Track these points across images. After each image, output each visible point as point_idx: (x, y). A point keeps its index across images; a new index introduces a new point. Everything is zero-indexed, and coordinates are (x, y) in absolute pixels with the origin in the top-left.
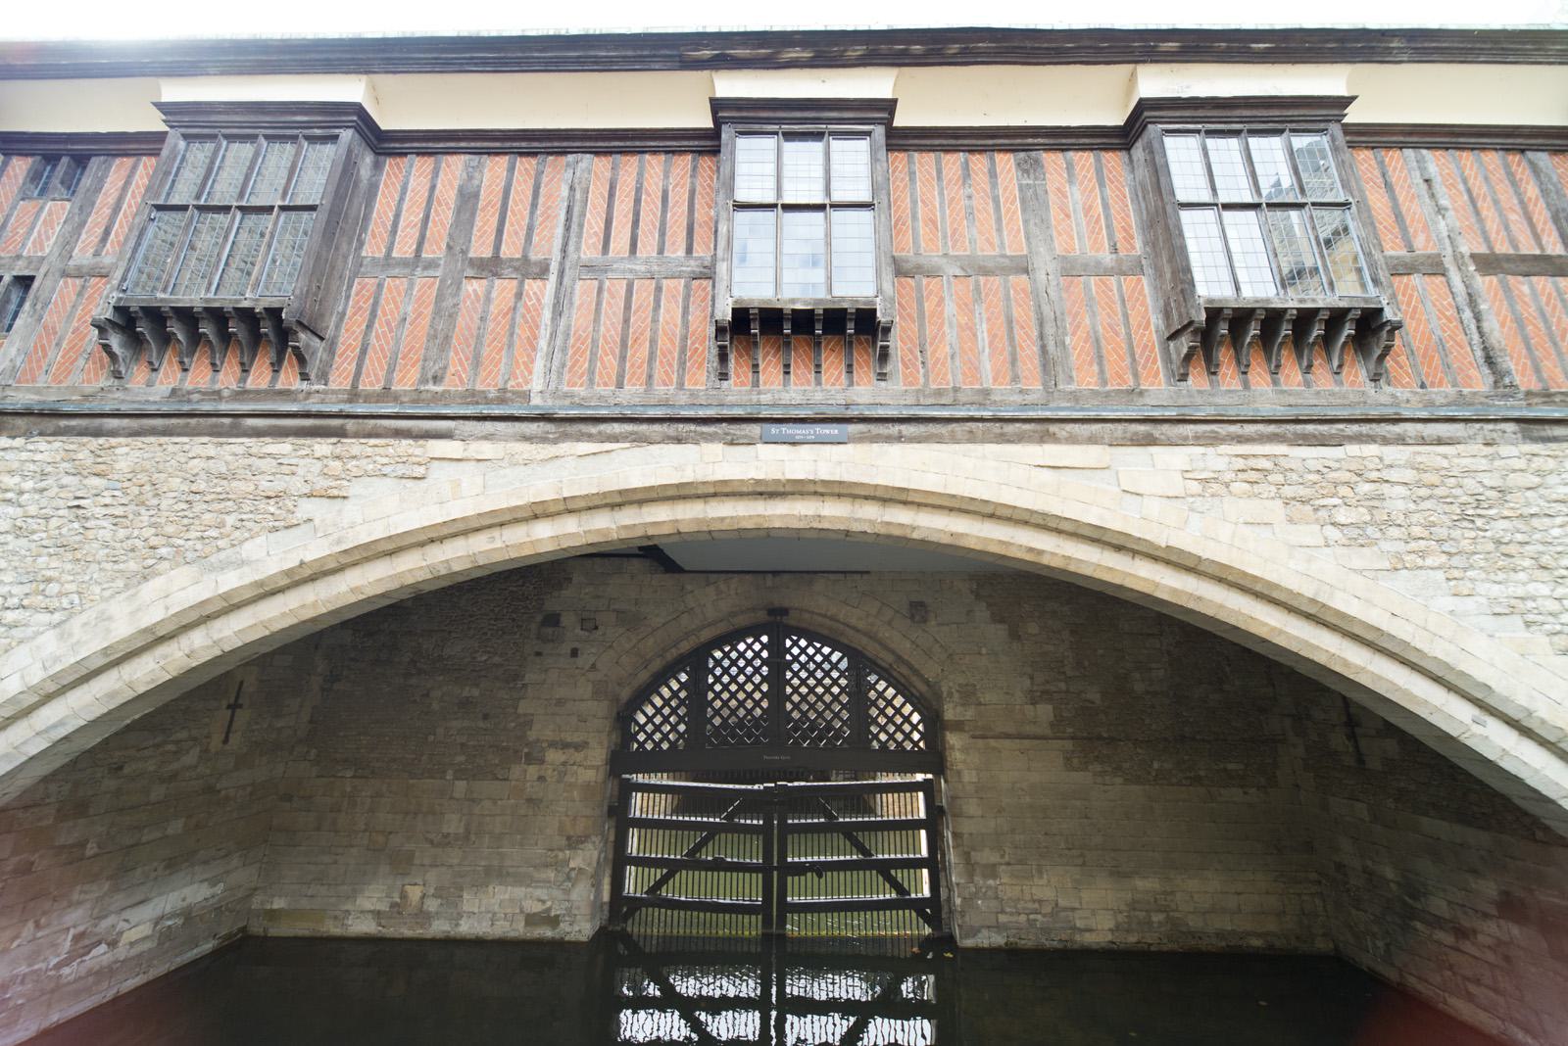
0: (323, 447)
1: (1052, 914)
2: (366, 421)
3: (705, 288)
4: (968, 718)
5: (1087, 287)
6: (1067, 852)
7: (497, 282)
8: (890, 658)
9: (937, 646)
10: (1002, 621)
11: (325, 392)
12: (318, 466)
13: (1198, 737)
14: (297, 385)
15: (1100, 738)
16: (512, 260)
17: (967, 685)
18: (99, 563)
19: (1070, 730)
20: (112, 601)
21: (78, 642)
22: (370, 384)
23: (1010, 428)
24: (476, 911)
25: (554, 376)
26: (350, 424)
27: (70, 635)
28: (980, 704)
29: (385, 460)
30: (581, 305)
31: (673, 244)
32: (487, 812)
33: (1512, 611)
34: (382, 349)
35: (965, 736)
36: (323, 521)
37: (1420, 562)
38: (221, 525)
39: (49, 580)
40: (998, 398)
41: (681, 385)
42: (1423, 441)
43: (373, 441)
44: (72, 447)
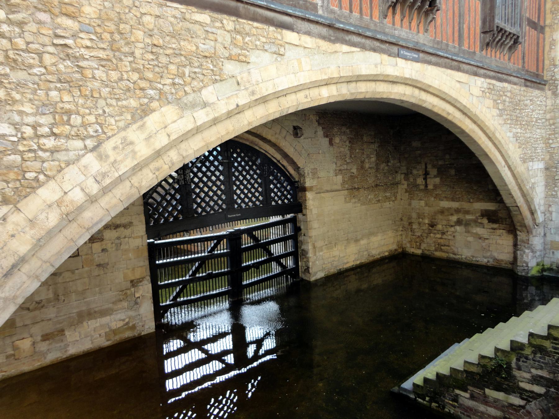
0: (229, 22)
1: (338, 260)
2: (249, 7)
4: (314, 185)
6: (344, 236)
8: (278, 156)
9: (303, 150)
10: (327, 136)
13: (380, 184)
15: (355, 188)
17: (314, 169)
18: (105, 99)
19: (347, 186)
20: (128, 130)
21: (115, 161)
24: (78, 339)
27: (107, 156)
28: (319, 178)
32: (68, 280)
35: (314, 193)
38: (182, 76)
39: (69, 113)
43: (256, 24)
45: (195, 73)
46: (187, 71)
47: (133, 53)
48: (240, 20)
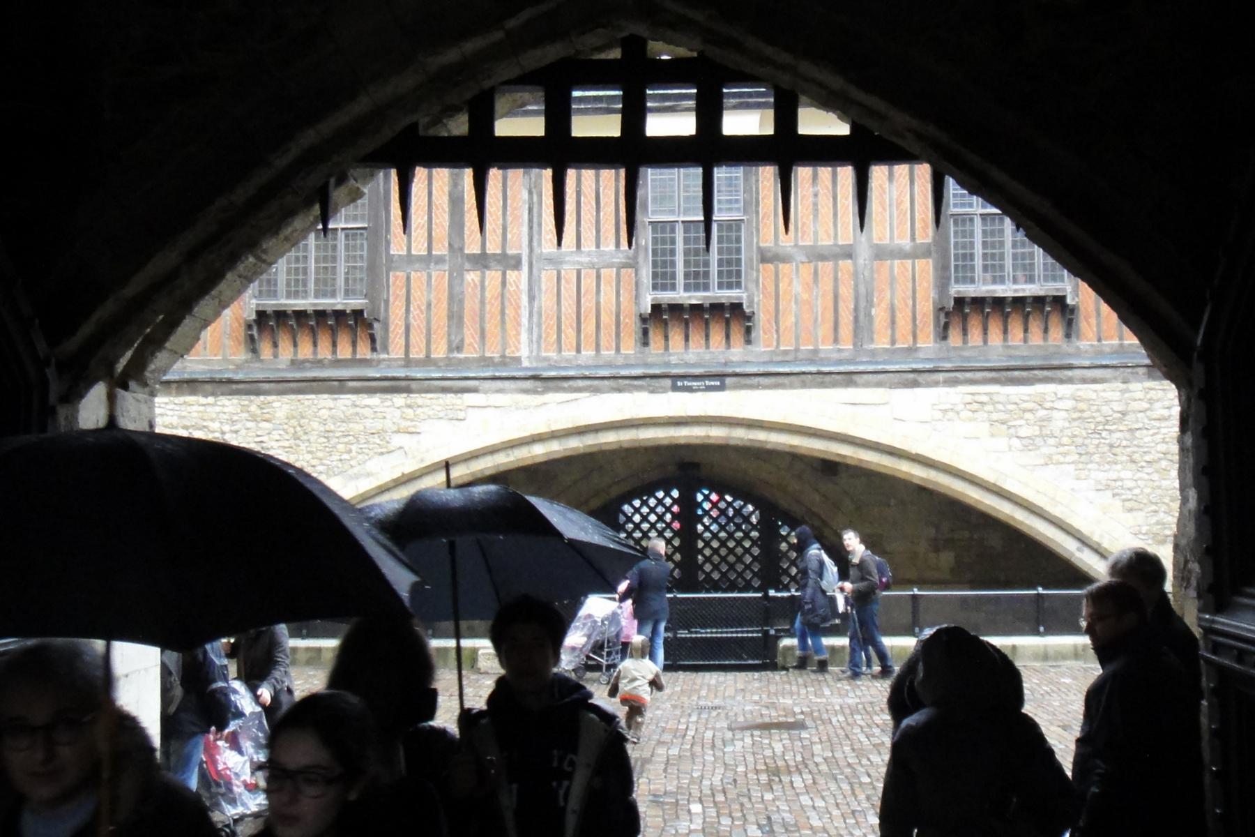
0: (399, 399)
3: (630, 276)
5: (891, 268)
7: (487, 273)
11: (389, 360)
12: (398, 413)
14: (369, 355)
16: (494, 254)
22: (417, 353)
23: (827, 378)
25: (535, 346)
26: (414, 385)
29: (440, 408)
30: (547, 290)
31: (606, 239)
33: (1108, 487)
34: (419, 327)
36: (410, 448)
37: (1062, 459)
38: (350, 451)
40: (822, 355)
41: (618, 349)
42: (1084, 381)
43: (429, 396)
44: (246, 403)
45: (361, 448)
46: (354, 448)
47: (309, 440)
48: (411, 395)
